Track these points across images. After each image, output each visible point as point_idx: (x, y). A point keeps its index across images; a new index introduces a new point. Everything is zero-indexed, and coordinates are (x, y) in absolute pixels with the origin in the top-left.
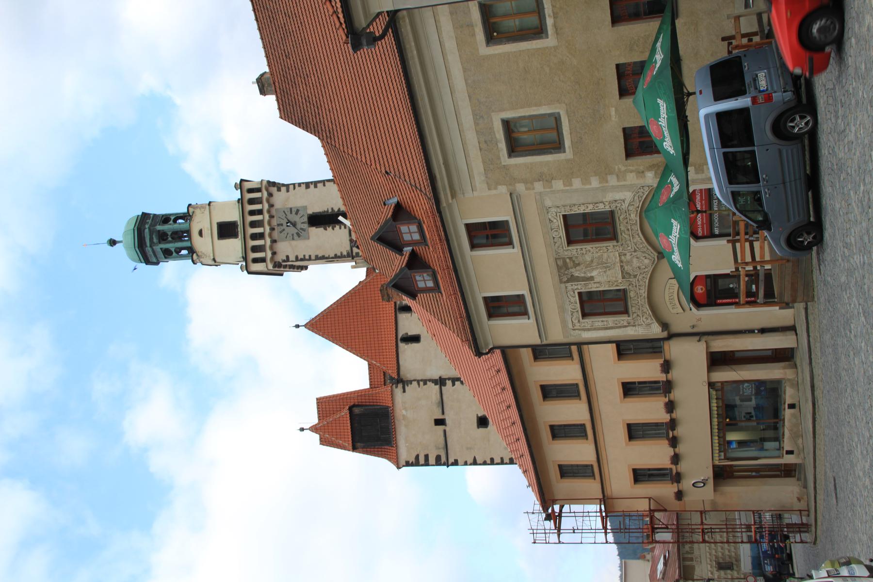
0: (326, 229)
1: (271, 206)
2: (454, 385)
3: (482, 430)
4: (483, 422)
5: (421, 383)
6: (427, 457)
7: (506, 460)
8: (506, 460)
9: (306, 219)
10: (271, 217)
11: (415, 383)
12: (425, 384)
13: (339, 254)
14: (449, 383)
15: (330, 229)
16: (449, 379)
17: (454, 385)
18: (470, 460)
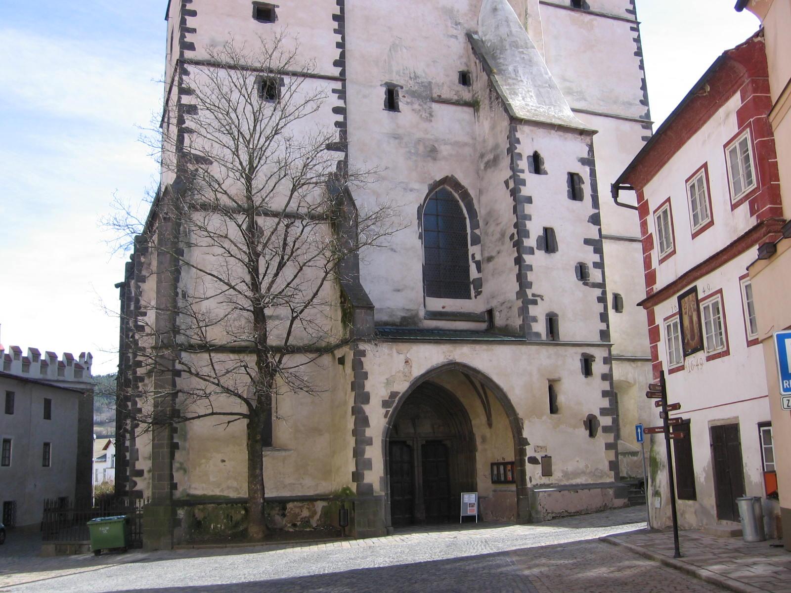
3: (250, 10)
7: (189, 38)
8: (189, 38)
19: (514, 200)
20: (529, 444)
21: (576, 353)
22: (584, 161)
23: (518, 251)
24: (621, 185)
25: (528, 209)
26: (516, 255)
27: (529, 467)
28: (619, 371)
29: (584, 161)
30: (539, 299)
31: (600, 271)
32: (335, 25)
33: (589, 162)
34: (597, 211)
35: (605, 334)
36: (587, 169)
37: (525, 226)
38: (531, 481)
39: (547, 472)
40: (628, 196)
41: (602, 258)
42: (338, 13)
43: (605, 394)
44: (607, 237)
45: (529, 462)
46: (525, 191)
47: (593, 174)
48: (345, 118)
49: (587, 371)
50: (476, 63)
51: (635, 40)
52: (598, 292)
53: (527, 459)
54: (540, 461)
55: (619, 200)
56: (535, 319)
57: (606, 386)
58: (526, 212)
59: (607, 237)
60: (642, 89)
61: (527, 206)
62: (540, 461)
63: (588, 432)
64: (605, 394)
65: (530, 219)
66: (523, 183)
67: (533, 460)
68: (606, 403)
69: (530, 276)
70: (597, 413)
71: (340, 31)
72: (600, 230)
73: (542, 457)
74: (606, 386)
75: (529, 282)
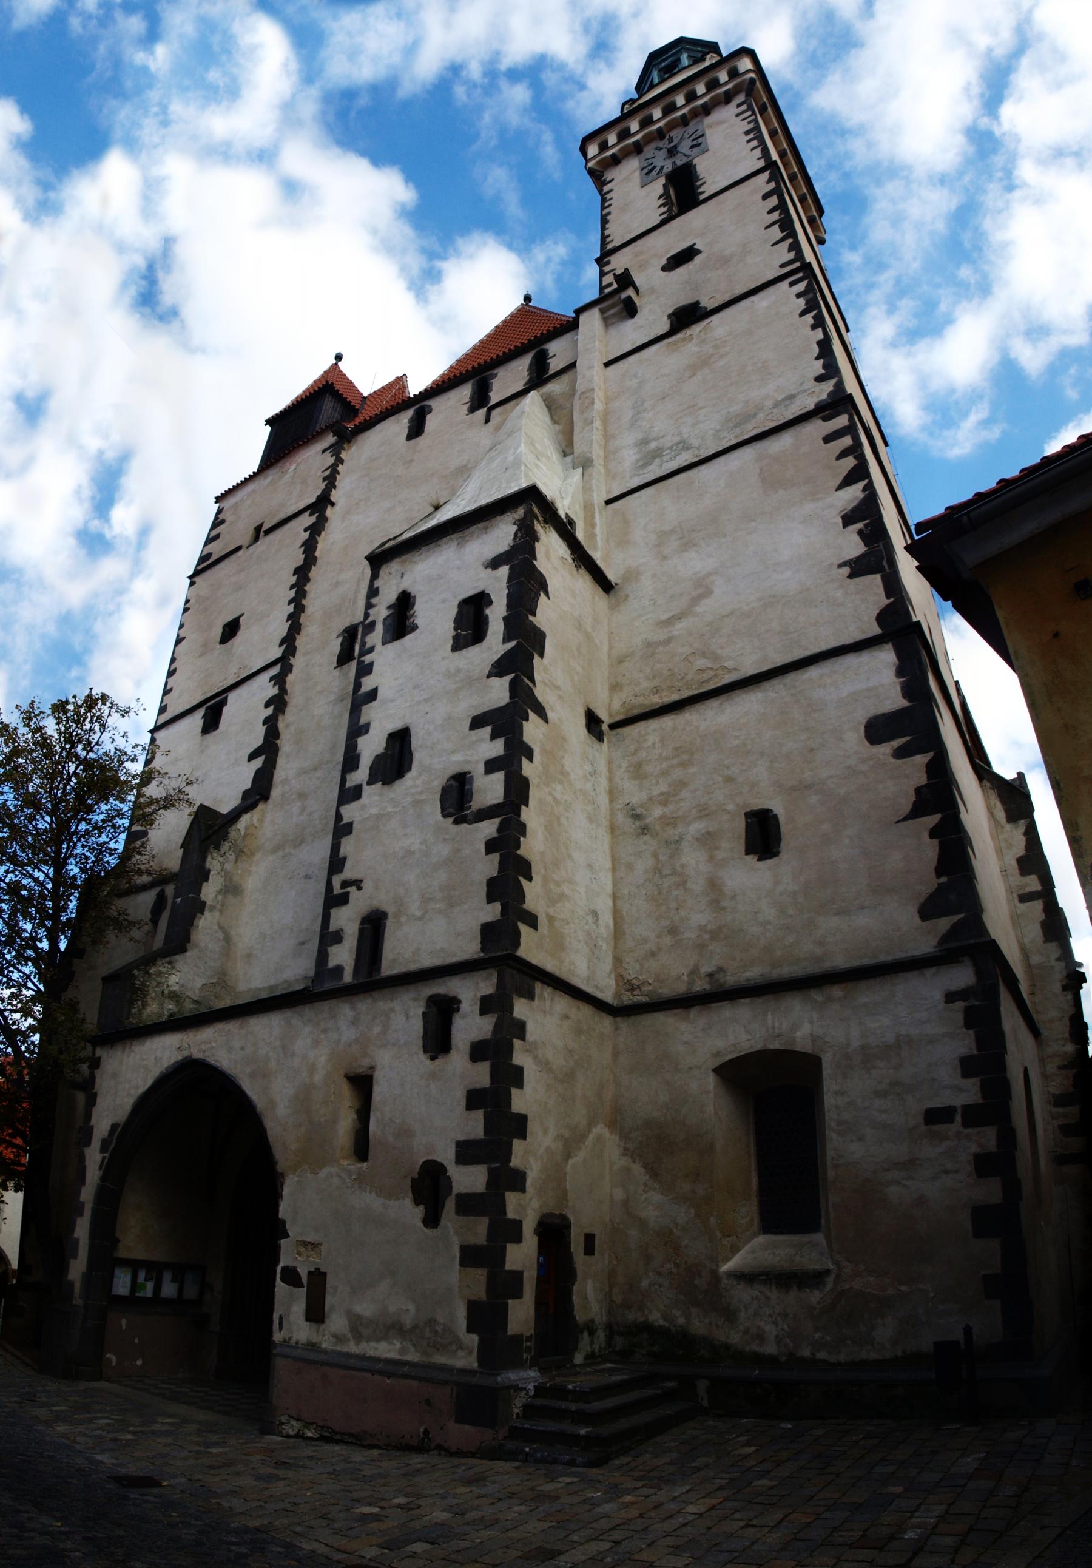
20: (288, 1236)
21: (415, 1000)
27: (281, 1288)
30: (352, 890)
38: (281, 1328)
39: (316, 1314)
45: (283, 1280)
49: (437, 1042)
52: (489, 828)
53: (279, 1269)
54: (304, 1280)
62: (304, 1280)
63: (419, 1212)
67: (291, 1277)
68: (474, 1126)
70: (446, 1155)
73: (310, 1273)
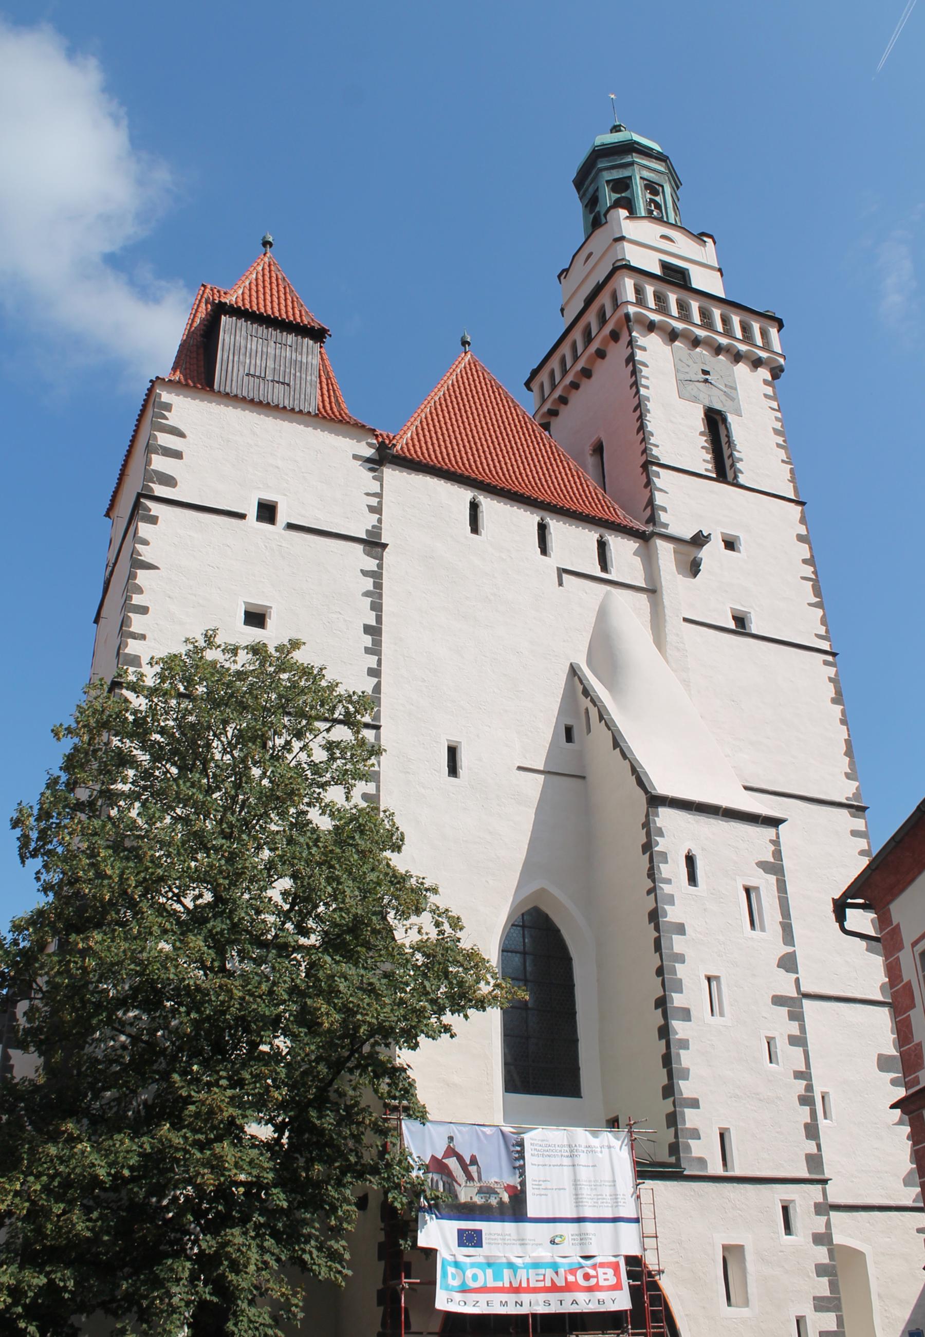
0: (702, 434)
1: (738, 357)
2: (365, 573)
4: (256, 618)
5: (374, 502)
6: (177, 455)
9: (718, 406)
10: (718, 350)
11: (375, 487)
12: (372, 509)
13: (653, 440)
14: (371, 564)
15: (703, 441)
16: (380, 566)
17: (365, 573)
18: (146, 553)
19: (657, 928)
22: (764, 866)
23: (665, 1015)
24: (849, 901)
25: (678, 944)
26: (662, 1022)
28: (847, 1231)
29: (764, 866)
31: (800, 1050)
32: (368, 640)
33: (775, 867)
34: (790, 949)
35: (815, 1161)
36: (772, 879)
37: (674, 972)
40: (861, 920)
41: (803, 1028)
42: (374, 623)
43: (821, 1270)
44: (807, 996)
46: (672, 914)
47: (782, 887)
48: (378, 788)
50: (587, 709)
51: (830, 679)
55: (848, 925)
56: (695, 1134)
57: (821, 1254)
58: (677, 949)
59: (807, 996)
60: (846, 754)
61: (676, 938)
64: (821, 1270)
65: (683, 961)
66: (671, 900)
68: (822, 1287)
69: (685, 1059)
71: (375, 650)
72: (797, 981)
74: (821, 1254)
75: (684, 1069)
